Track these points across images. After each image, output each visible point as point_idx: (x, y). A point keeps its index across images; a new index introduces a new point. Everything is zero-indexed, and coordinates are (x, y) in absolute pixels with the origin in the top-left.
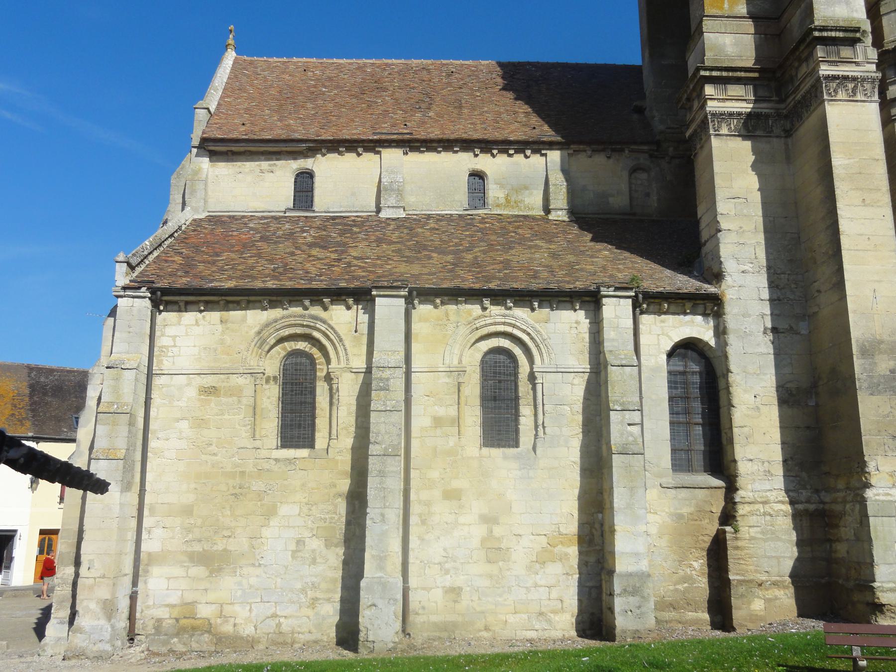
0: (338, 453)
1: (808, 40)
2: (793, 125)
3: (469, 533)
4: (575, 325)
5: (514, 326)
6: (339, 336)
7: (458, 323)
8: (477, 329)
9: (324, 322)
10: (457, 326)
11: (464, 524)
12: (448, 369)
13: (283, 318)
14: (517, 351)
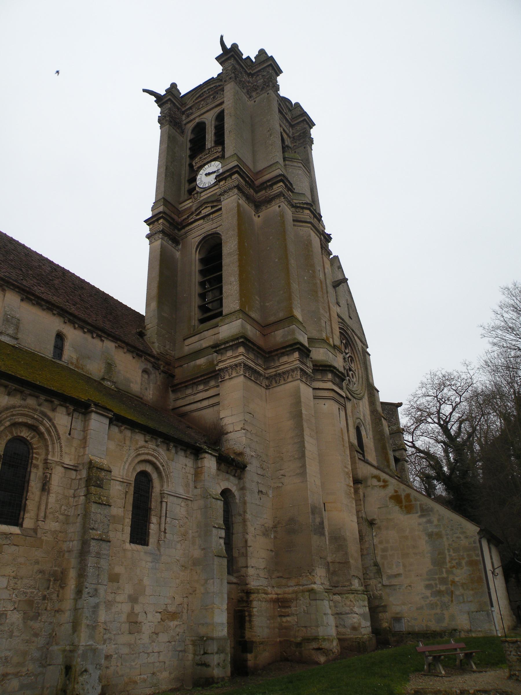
0: (44, 533)
1: (294, 347)
2: (271, 384)
3: (121, 609)
4: (184, 467)
5: (156, 458)
6: (58, 435)
7: (130, 447)
8: (139, 455)
9: (50, 420)
10: (129, 450)
11: (119, 602)
12: (122, 480)
13: (19, 407)
14: (154, 476)
